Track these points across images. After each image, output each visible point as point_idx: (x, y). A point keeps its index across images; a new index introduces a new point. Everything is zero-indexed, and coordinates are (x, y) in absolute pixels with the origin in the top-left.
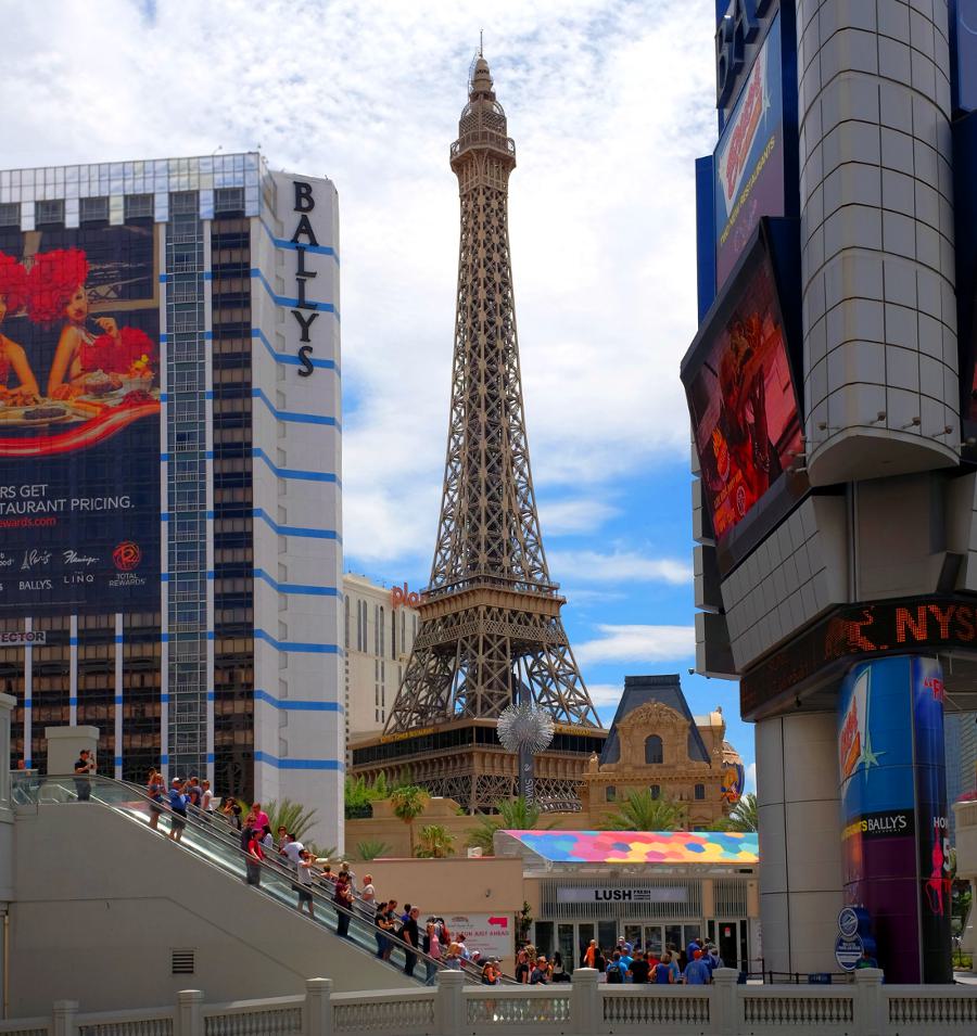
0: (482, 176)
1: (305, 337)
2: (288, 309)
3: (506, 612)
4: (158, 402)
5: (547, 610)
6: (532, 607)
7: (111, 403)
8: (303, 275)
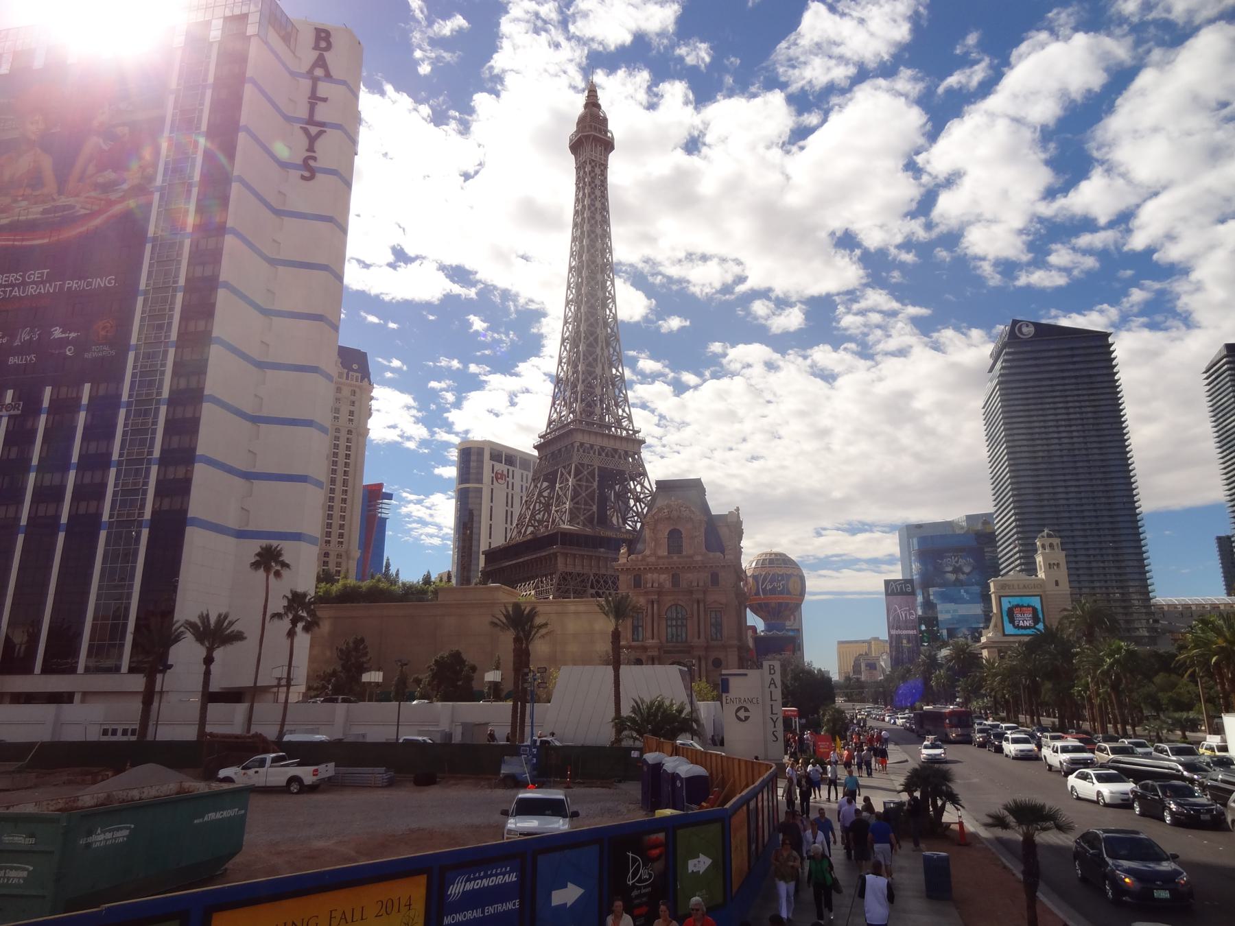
0: (588, 152)
1: (311, 148)
2: (297, 126)
3: (596, 448)
4: (152, 193)
5: (630, 447)
6: (618, 445)
7: (113, 196)
8: (315, 99)
